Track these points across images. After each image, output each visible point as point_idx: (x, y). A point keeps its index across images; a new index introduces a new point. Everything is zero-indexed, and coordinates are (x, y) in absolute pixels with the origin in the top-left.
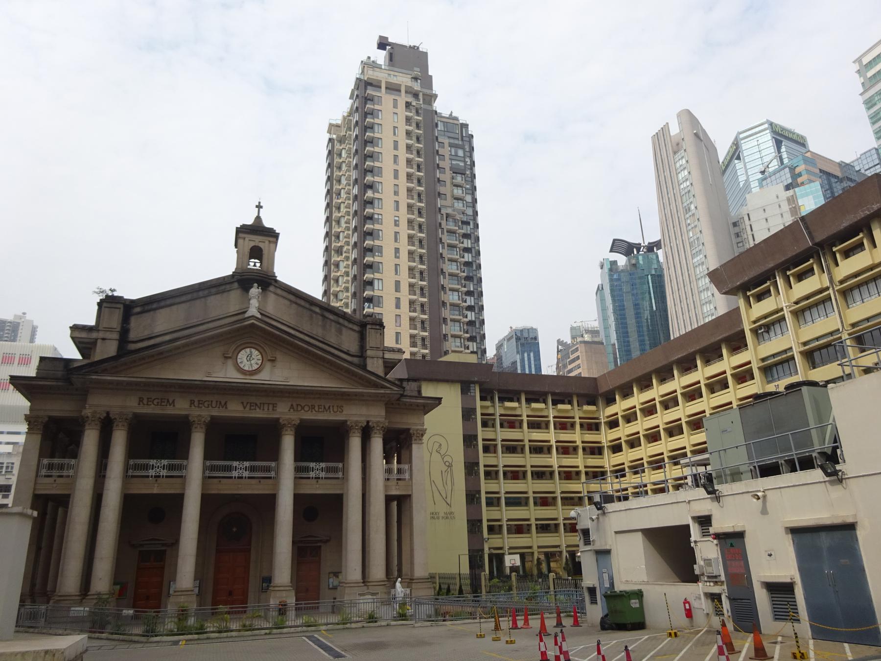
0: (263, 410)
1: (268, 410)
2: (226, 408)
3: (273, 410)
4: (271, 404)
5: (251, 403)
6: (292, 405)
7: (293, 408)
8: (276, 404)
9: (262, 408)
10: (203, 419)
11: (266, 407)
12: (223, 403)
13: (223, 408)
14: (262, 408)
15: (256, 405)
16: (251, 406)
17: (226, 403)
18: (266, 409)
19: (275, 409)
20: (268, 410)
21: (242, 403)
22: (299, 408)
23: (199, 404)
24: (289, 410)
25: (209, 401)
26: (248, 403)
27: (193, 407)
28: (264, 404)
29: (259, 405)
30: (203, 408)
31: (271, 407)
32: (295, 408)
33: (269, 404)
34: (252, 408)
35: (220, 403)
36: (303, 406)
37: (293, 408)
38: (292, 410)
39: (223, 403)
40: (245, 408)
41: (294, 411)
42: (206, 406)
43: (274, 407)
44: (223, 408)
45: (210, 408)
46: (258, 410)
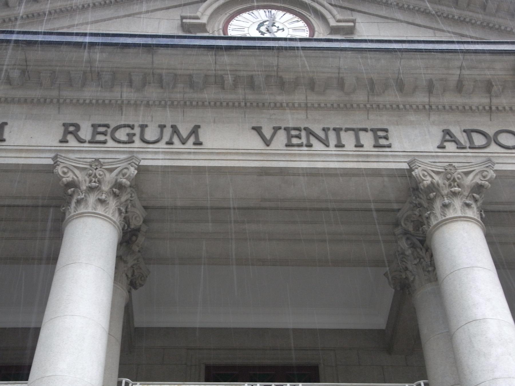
0: (340, 145)
1: (359, 145)
2: (198, 143)
3: (377, 146)
4: (365, 130)
5: (287, 129)
6: (447, 132)
7: (455, 141)
8: (386, 130)
9: (333, 141)
10: (110, 178)
11: (348, 139)
12: (184, 131)
13: (184, 142)
14: (333, 141)
15: (310, 133)
16: (290, 137)
17: (195, 131)
18: (348, 139)
19: (382, 142)
20: (359, 145)
21: (258, 130)
22: (479, 140)
23: (95, 133)
24: (441, 147)
25: (132, 127)
26: (276, 129)
27: (72, 142)
28: (337, 131)
29: (322, 135)
30: (111, 143)
31: (367, 139)
32: (462, 138)
33: (356, 131)
34: (295, 141)
35: (175, 130)
36: (491, 132)
37: (455, 141)
38: (451, 147)
39: (184, 131)
40: (267, 143)
41: (461, 147)
42: (124, 138)
43: (377, 138)
44: (184, 142)
45: (138, 143)
46: (318, 146)
